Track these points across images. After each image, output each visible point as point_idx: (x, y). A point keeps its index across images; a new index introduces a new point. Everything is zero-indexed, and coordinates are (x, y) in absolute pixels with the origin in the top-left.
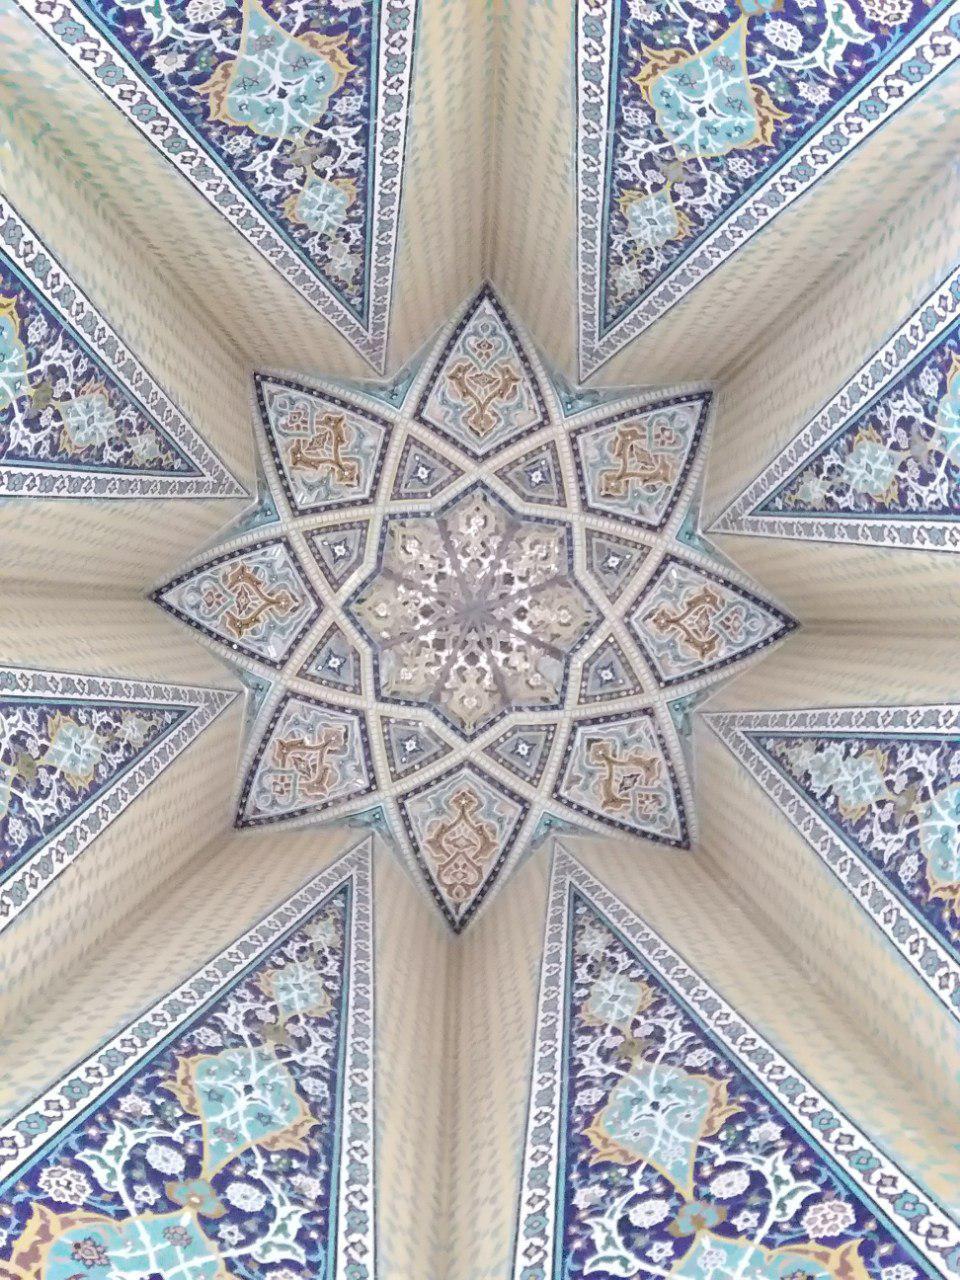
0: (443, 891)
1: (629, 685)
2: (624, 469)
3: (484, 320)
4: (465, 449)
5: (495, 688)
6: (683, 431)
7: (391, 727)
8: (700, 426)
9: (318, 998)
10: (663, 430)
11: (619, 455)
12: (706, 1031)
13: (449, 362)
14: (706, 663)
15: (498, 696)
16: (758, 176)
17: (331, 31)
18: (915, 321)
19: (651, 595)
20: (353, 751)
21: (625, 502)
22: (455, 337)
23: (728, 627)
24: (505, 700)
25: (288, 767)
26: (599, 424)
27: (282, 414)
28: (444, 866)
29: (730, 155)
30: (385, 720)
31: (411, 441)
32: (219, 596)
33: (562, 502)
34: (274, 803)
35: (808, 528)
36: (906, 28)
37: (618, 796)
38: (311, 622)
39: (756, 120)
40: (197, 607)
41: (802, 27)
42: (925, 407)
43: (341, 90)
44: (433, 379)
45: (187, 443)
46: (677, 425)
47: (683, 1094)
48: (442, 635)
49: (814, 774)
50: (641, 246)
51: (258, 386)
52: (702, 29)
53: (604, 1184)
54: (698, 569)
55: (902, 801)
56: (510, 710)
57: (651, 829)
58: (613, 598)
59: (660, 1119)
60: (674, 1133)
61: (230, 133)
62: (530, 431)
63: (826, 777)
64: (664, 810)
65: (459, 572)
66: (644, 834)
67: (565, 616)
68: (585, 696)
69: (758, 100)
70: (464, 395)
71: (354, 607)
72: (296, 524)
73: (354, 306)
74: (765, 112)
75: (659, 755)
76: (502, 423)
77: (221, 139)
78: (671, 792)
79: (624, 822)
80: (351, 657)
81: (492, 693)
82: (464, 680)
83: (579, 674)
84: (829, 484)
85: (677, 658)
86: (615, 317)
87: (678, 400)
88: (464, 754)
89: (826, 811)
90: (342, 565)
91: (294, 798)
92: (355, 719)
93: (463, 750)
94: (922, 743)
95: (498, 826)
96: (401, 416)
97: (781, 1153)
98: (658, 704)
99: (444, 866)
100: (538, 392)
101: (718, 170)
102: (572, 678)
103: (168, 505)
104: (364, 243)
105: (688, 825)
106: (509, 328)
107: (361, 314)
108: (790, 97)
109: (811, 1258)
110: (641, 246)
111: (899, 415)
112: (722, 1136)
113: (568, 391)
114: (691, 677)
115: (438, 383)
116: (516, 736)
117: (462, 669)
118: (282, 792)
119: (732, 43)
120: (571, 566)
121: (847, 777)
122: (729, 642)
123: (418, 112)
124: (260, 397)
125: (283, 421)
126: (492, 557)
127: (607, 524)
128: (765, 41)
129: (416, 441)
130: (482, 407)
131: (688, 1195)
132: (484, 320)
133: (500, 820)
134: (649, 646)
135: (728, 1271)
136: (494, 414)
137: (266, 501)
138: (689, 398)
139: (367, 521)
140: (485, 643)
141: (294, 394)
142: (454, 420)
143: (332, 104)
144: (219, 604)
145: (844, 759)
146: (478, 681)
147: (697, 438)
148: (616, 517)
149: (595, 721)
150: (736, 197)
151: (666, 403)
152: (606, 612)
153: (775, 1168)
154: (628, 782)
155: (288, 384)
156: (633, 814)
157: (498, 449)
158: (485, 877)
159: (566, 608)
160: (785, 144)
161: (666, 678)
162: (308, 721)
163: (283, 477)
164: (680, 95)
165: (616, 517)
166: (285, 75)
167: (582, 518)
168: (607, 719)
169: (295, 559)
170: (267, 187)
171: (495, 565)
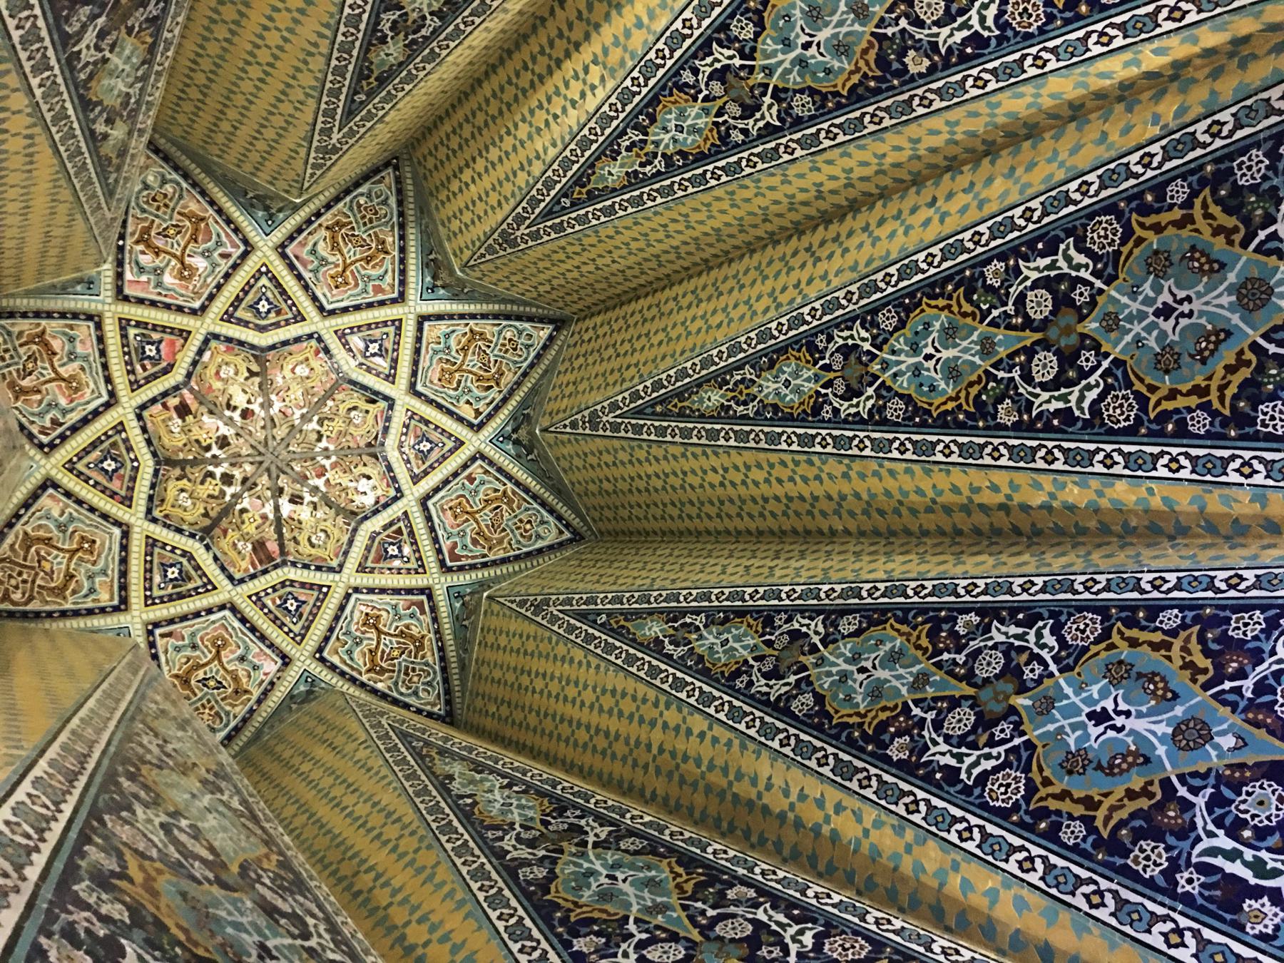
1: (296, 629)
3: (534, 333)
4: (414, 374)
5: (213, 514)
6: (539, 537)
7: (117, 438)
8: (551, 547)
14: (364, 678)
15: (207, 522)
16: (898, 424)
17: (882, 62)
18: (882, 586)
19: (387, 598)
20: (72, 410)
22: (508, 317)
23: (406, 674)
25: (22, 351)
26: (500, 470)
27: (369, 196)
28: (11, 562)
29: (901, 396)
30: (120, 428)
31: (398, 324)
32: (166, 206)
35: (610, 648)
36: (1111, 432)
38: (180, 309)
39: (951, 391)
41: (1062, 371)
42: (827, 635)
43: (818, 92)
44: (462, 316)
45: (384, 100)
46: (540, 530)
48: (233, 441)
50: (755, 390)
51: (387, 164)
52: (1010, 316)
54: (435, 620)
56: (202, 539)
58: (362, 569)
61: (755, 18)
62: (460, 420)
67: (319, 538)
68: (259, 599)
69: (971, 384)
72: (269, 253)
73: (559, 202)
74: (963, 394)
75: (256, 693)
77: (748, 10)
78: (232, 724)
80: (164, 364)
81: (206, 515)
82: (202, 483)
84: (671, 632)
86: (654, 413)
87: (559, 518)
88: (133, 520)
90: (247, 316)
92: (105, 398)
93: (135, 516)
95: (84, 591)
96: (415, 305)
99: (11, 562)
100: (497, 409)
101: (879, 396)
102: (267, 576)
103: (312, 103)
104: (643, 180)
106: (538, 356)
107: (548, 214)
108: (991, 401)
110: (755, 390)
111: (797, 626)
113: (515, 430)
114: (343, 674)
117: (211, 475)
119: (1005, 341)
121: (498, 797)
123: (804, 166)
124: (376, 171)
126: (332, 447)
128: (1030, 360)
129: (399, 328)
132: (534, 333)
133: (92, 591)
137: (281, 215)
138: (568, 526)
139: (304, 319)
140: (248, 484)
141: (393, 201)
143: (802, 91)
144: (158, 208)
146: (210, 496)
149: (243, 620)
150: (863, 421)
151: (551, 511)
152: (345, 570)
154: (212, 683)
155: (400, 192)
158: (29, 607)
159: (328, 536)
160: (945, 422)
161: (325, 654)
163: (309, 222)
164: (935, 335)
166: (827, 40)
168: (253, 629)
169: (235, 267)
170: (695, 71)
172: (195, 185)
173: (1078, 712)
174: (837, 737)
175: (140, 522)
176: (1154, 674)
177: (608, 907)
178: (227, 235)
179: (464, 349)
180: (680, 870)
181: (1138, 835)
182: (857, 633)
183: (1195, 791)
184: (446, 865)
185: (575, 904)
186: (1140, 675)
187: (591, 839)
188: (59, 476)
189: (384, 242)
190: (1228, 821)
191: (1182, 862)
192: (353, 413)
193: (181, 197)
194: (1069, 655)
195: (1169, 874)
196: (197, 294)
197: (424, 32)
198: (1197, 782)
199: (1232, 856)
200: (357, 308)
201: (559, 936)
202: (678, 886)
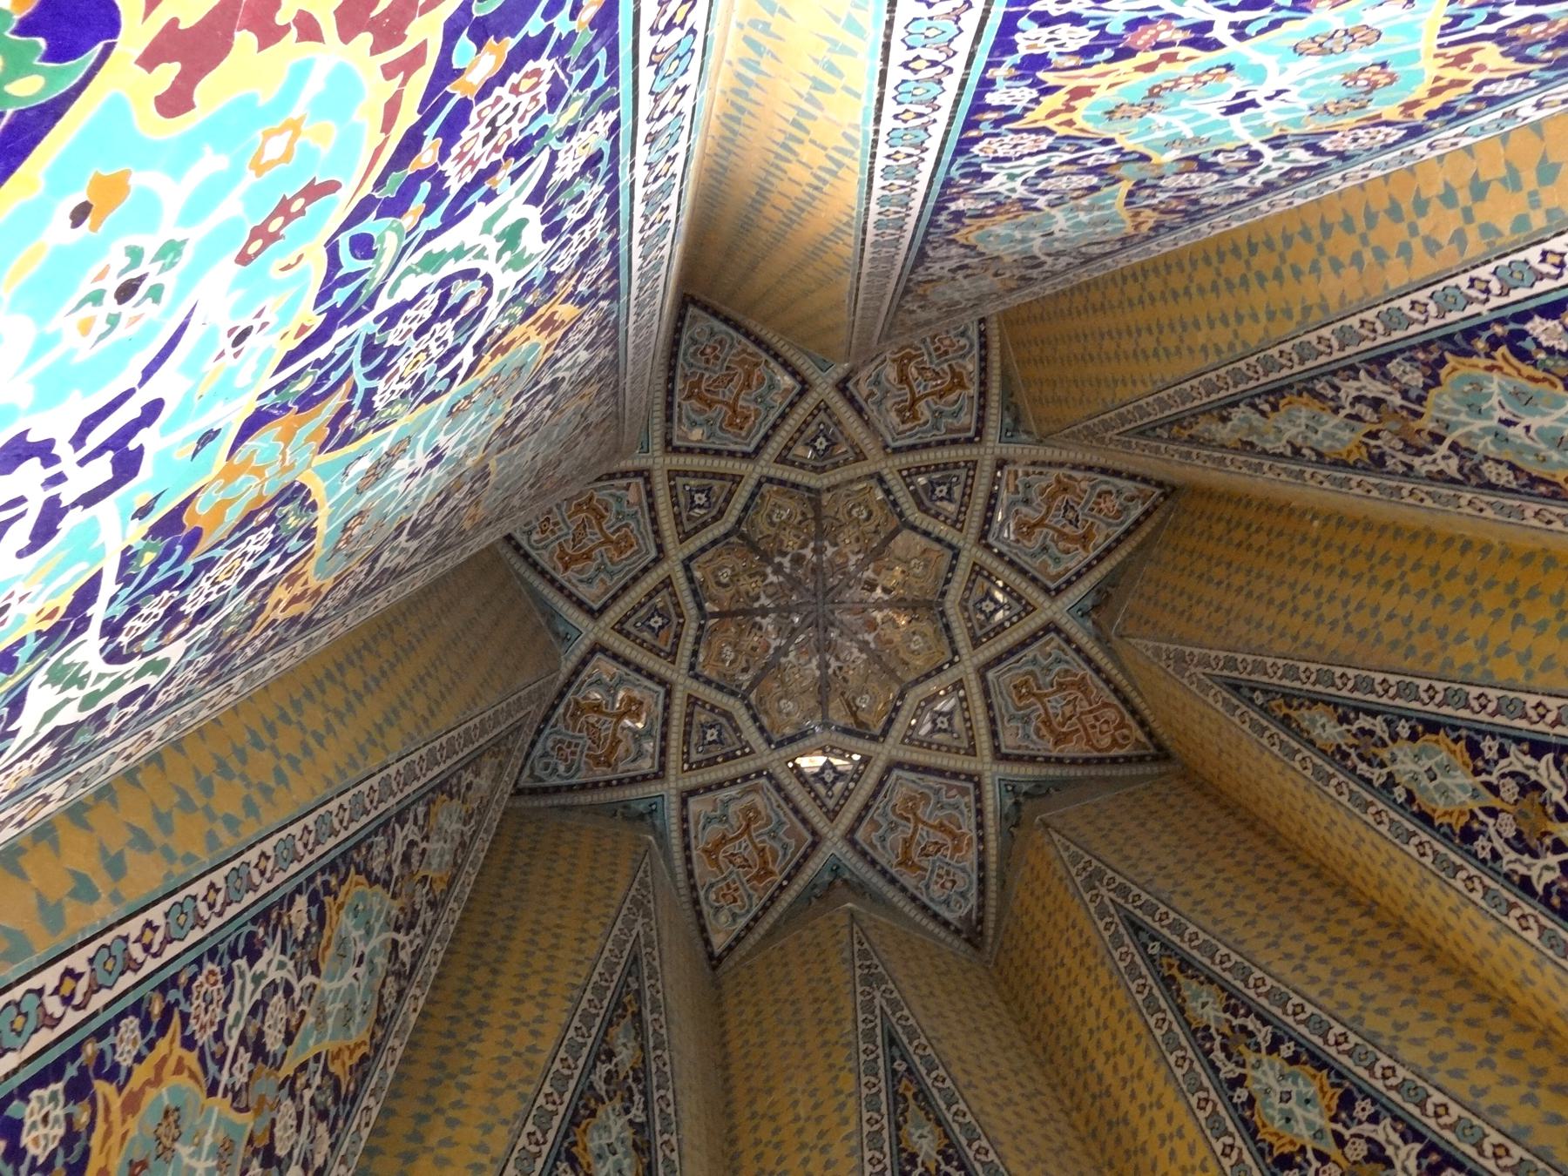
0: (1115, 752)
2: (727, 404)
4: (646, 570)
9: (1307, 1084)
10: (703, 353)
11: (710, 406)
12: (1554, 740)
13: (548, 568)
14: (973, 390)
20: (930, 788)
21: (763, 413)
23: (946, 353)
24: (929, 605)
25: (924, 864)
27: (555, 770)
32: (728, 886)
33: (737, 480)
34: (963, 895)
37: (1081, 532)
40: (734, 916)
44: (561, 589)
46: (704, 339)
49: (1254, 439)
56: (940, 604)
57: (1136, 511)
64: (1119, 492)
65: (773, 610)
66: (1138, 523)
67: (860, 513)
68: (957, 521)
70: (589, 558)
71: (776, 737)
72: (672, 778)
75: (1055, 472)
76: (633, 525)
79: (1114, 536)
83: (929, 519)
85: (955, 415)
88: (970, 670)
91: (963, 870)
92: (896, 773)
95: (1065, 666)
96: (590, 631)
98: (997, 451)
102: (930, 528)
105: (1148, 473)
114: (982, 407)
115: (567, 585)
116: (971, 607)
118: (954, 882)
120: (809, 489)
122: (963, 356)
125: (562, 768)
126: (769, 570)
127: (778, 439)
129: (621, 622)
130: (608, 541)
133: (1058, 661)
134: (928, 438)
136: (618, 530)
139: (690, 696)
142: (612, 574)
143: (377, 880)
144: (736, 890)
147: (726, 320)
148: (775, 427)
152: (873, 469)
154: (1071, 515)
156: (1109, 525)
157: (657, 533)
158: (1116, 702)
161: (971, 434)
162: (885, 826)
163: (620, 782)
165: (775, 427)
167: (762, 463)
171: (778, 569)
172: (693, 888)
175: (968, 663)
178: (697, 823)
179: (588, 556)
188: (986, 752)
189: (573, 715)
192: (725, 580)
193: (712, 885)
196: (755, 790)
197: (602, 1069)
200: (638, 669)
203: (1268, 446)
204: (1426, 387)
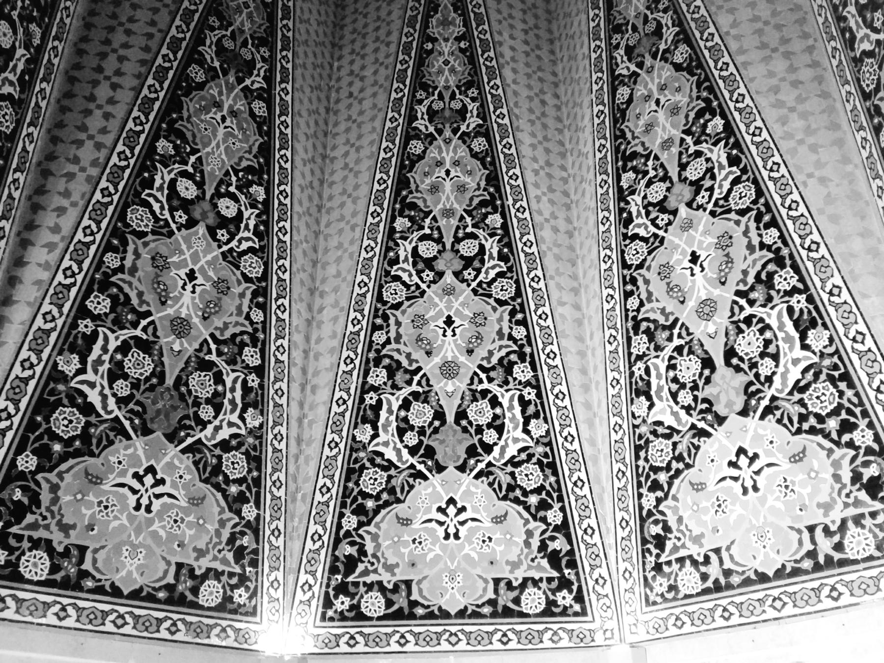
47: (240, 128)
49: (439, 15)
53: (175, 147)
55: (447, 113)
59: (221, 131)
60: (222, 148)
63: (440, 29)
89: (422, 48)
94: (482, 105)
97: (257, 211)
109: (234, 278)
112: (241, 174)
131: (208, 197)
135: (201, 255)
145: (456, 39)
153: (249, 218)
173: (690, 247)
174: (616, 138)
176: (732, 262)
177: (428, 198)
180: (483, 184)
181: (647, 332)
182: (678, 67)
183: (680, 336)
184: (381, 115)
185: (417, 186)
186: (727, 255)
187: (463, 128)
190: (673, 362)
191: (646, 359)
194: (722, 206)
195: (639, 358)
198: (684, 333)
199: (659, 376)
201: (394, 210)
202: (471, 199)
203: (434, 20)
204: (471, 150)
